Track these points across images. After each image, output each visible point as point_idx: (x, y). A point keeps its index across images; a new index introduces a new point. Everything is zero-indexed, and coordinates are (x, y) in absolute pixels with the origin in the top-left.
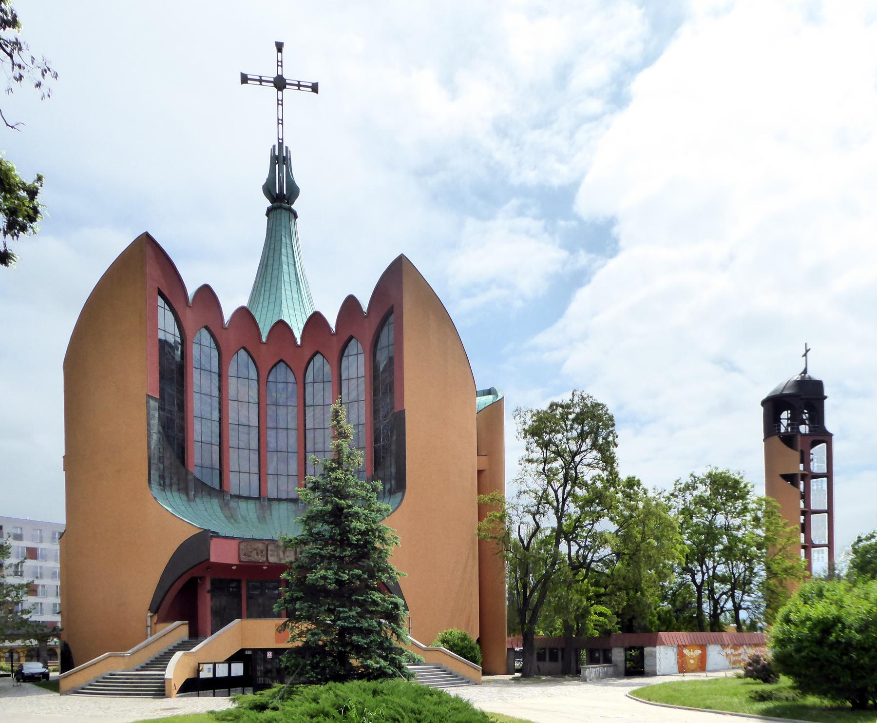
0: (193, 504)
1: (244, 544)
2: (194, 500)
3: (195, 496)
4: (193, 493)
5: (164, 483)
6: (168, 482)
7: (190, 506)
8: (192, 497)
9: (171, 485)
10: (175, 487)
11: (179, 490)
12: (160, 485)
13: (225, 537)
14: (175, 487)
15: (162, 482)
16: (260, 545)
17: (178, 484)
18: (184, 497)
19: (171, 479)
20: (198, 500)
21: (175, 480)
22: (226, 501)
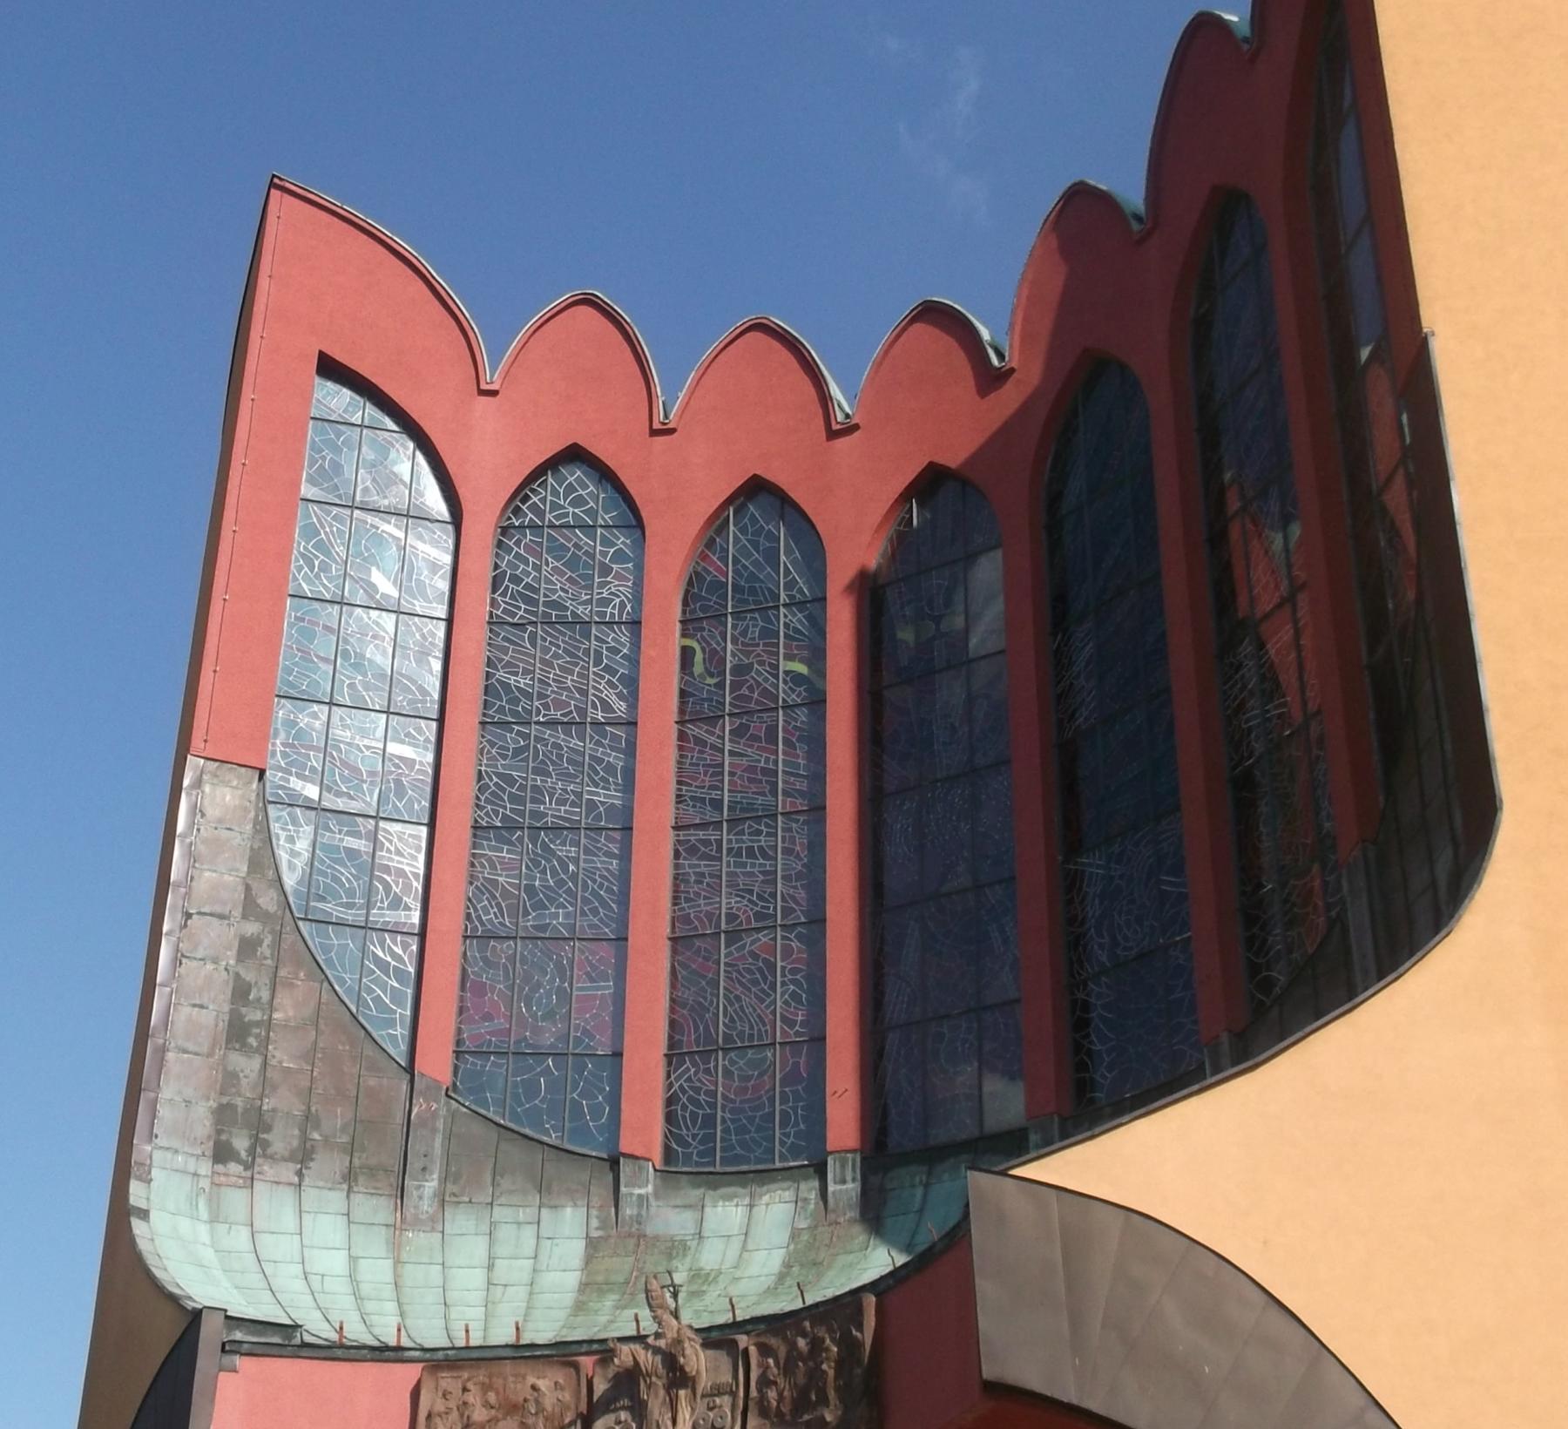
0: (419, 1241)
1: (448, 1381)
2: (435, 1223)
3: (442, 1201)
4: (431, 1185)
5: (259, 1147)
6: (282, 1139)
7: (396, 1249)
8: (427, 1206)
9: (303, 1156)
10: (328, 1164)
11: (349, 1178)
12: (222, 1153)
13: (338, 1351)
14: (328, 1164)
15: (241, 1143)
16: (543, 1384)
17: (351, 1149)
18: (374, 1207)
19: (309, 1120)
20: (461, 1221)
21: (336, 1119)
22: (628, 1211)
